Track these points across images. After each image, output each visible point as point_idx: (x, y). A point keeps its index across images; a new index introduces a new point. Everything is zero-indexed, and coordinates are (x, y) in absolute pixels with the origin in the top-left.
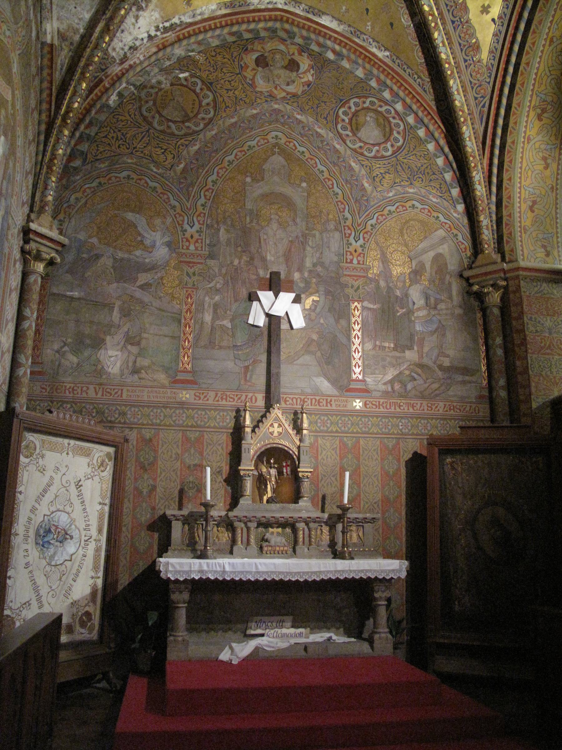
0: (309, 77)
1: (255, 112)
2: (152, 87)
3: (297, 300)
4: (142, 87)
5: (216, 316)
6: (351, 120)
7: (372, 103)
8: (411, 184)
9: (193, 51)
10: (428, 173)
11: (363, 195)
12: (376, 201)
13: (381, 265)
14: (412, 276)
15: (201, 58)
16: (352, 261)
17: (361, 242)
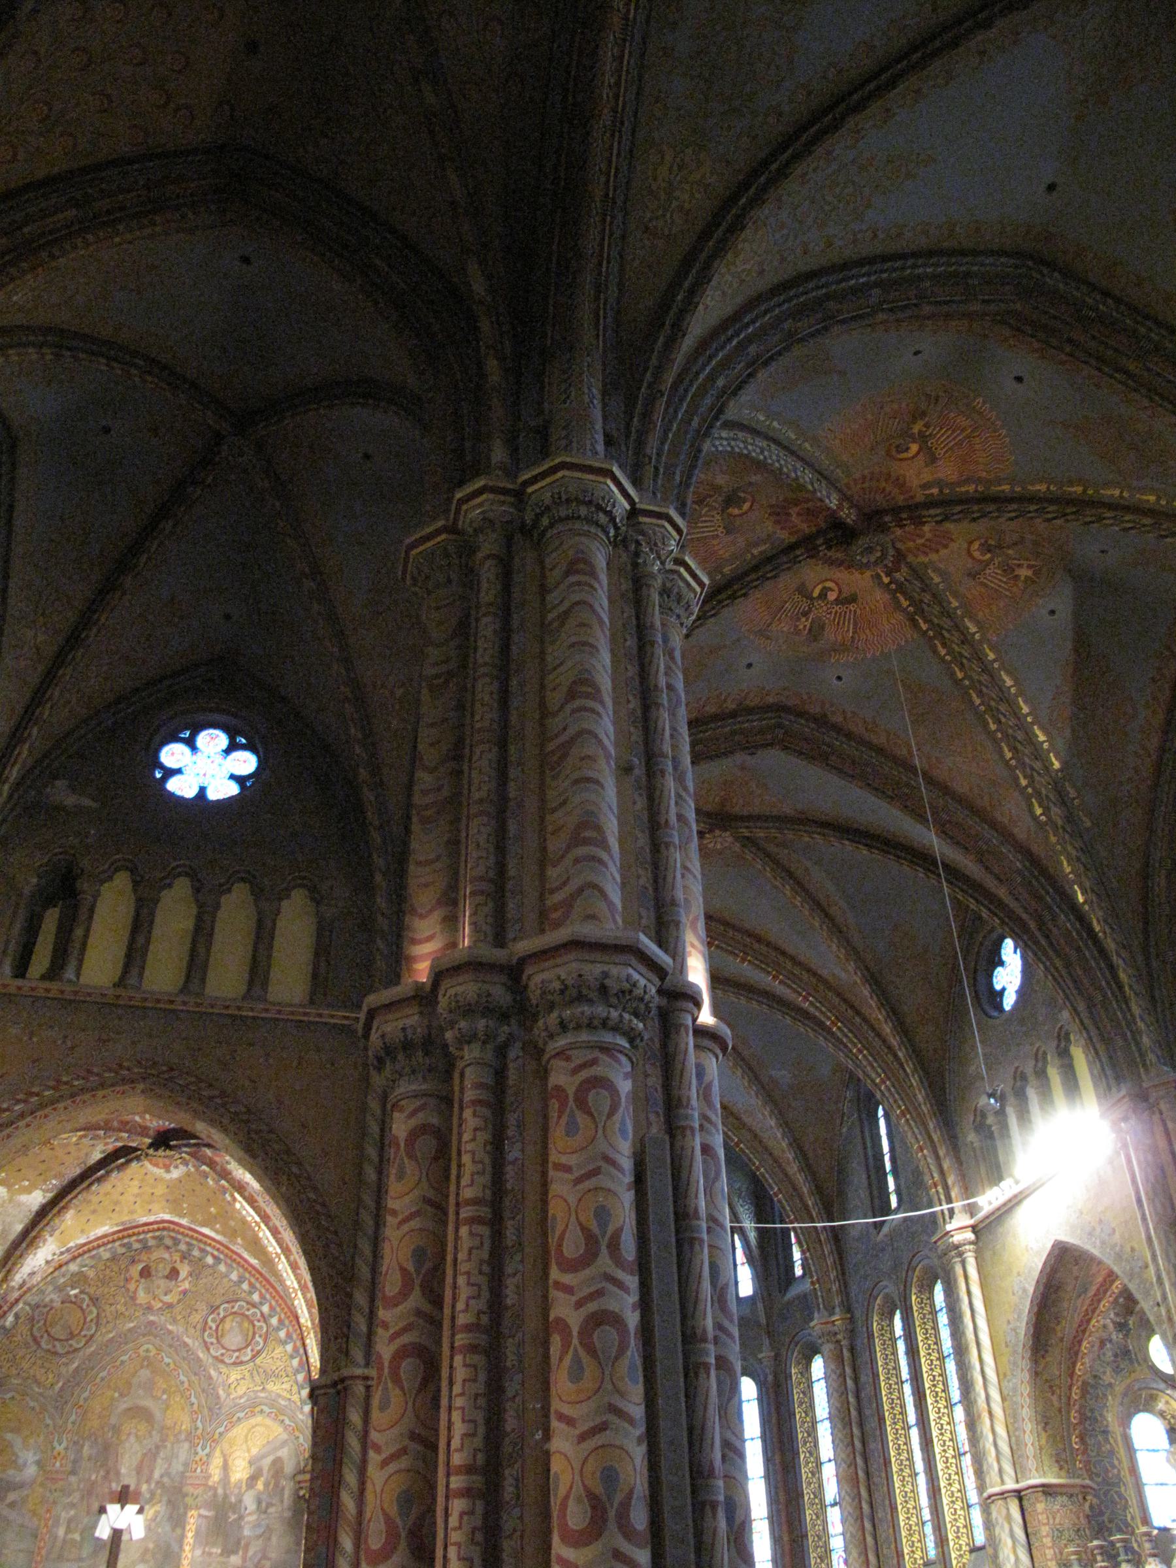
0: (186, 1285)
1: (132, 1325)
2: (45, 1306)
3: (140, 1511)
4: (37, 1306)
5: (68, 1530)
6: (217, 1327)
7: (241, 1307)
9: (86, 1266)
15: (91, 1274)
17: (207, 1450)
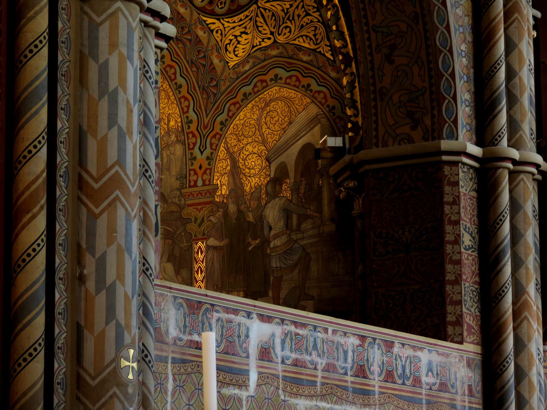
8: (275, 41)
10: (299, 16)
11: (212, 79)
12: (228, 84)
13: (231, 181)
14: (269, 188)
16: (196, 182)
